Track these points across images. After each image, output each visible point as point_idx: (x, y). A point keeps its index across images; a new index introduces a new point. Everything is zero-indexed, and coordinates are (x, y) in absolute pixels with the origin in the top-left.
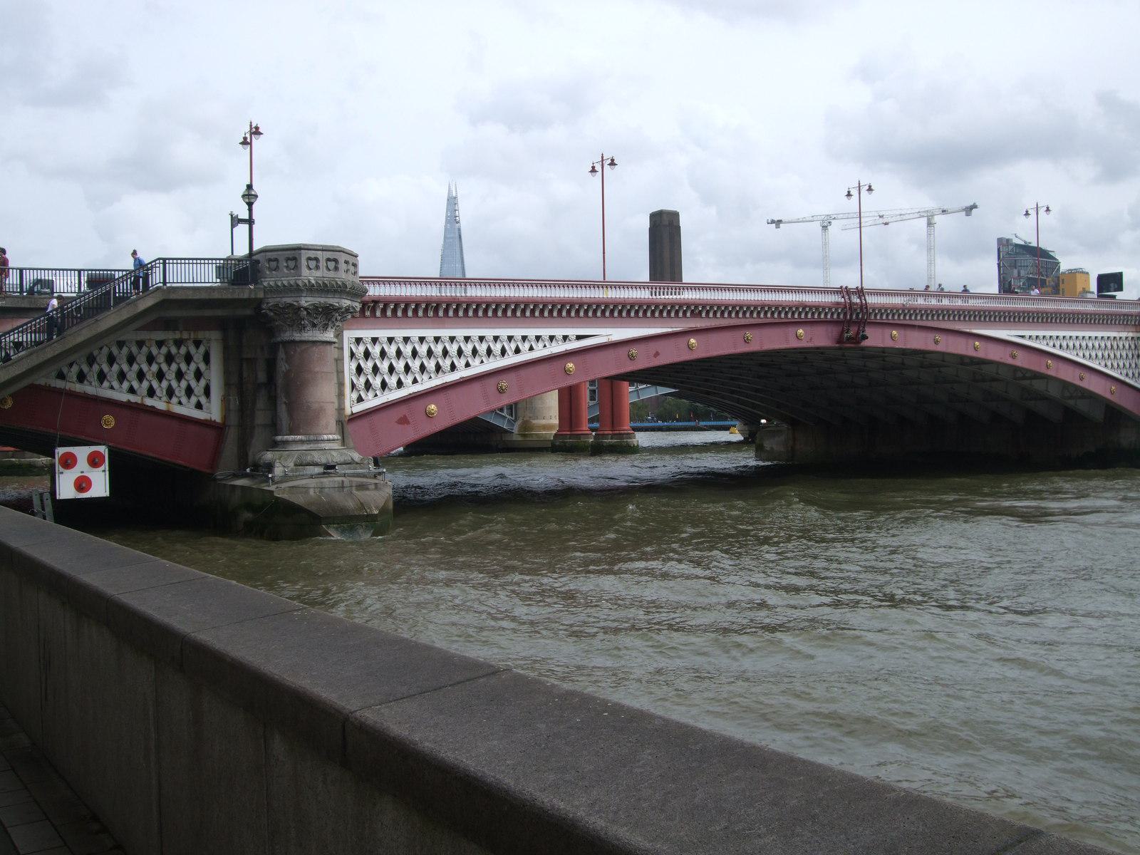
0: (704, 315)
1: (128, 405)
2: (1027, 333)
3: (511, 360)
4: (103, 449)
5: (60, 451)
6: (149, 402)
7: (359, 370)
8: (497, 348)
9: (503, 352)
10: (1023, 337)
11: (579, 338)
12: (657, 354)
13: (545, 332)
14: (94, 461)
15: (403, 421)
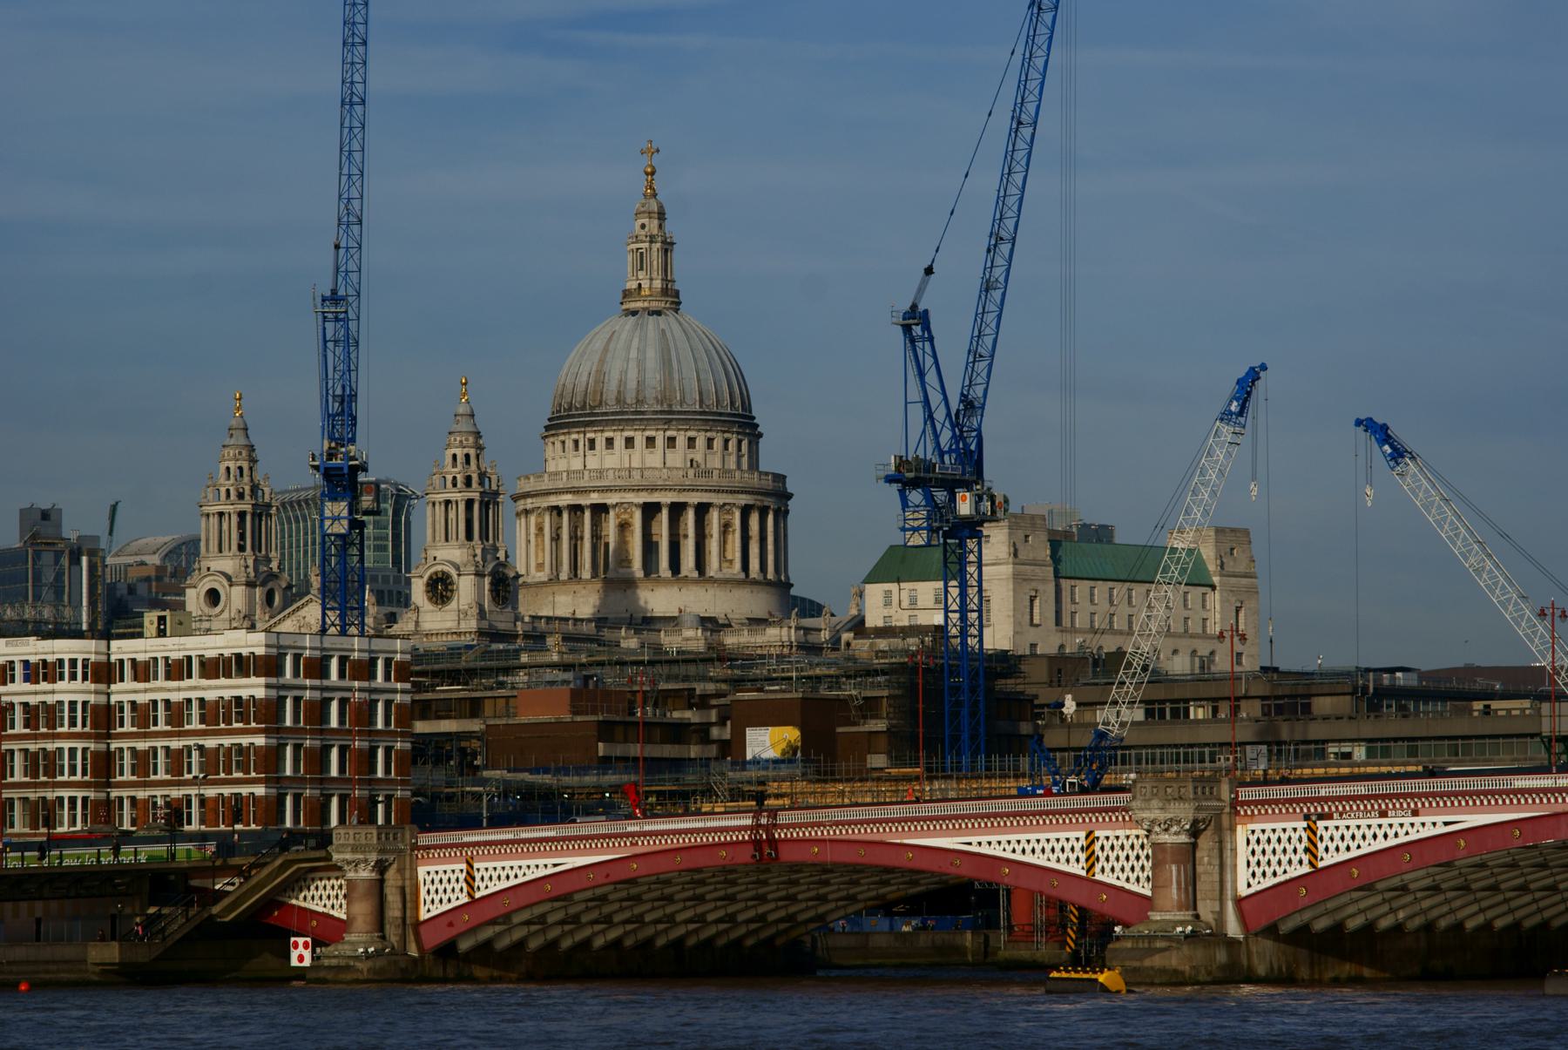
0: (640, 843)
1: (323, 914)
2: (974, 839)
3: (513, 882)
4: (309, 939)
5: (293, 939)
6: (332, 912)
7: (428, 892)
8: (503, 875)
9: (508, 877)
10: (970, 844)
11: (555, 865)
12: (608, 876)
13: (532, 862)
14: (306, 946)
15: (451, 925)
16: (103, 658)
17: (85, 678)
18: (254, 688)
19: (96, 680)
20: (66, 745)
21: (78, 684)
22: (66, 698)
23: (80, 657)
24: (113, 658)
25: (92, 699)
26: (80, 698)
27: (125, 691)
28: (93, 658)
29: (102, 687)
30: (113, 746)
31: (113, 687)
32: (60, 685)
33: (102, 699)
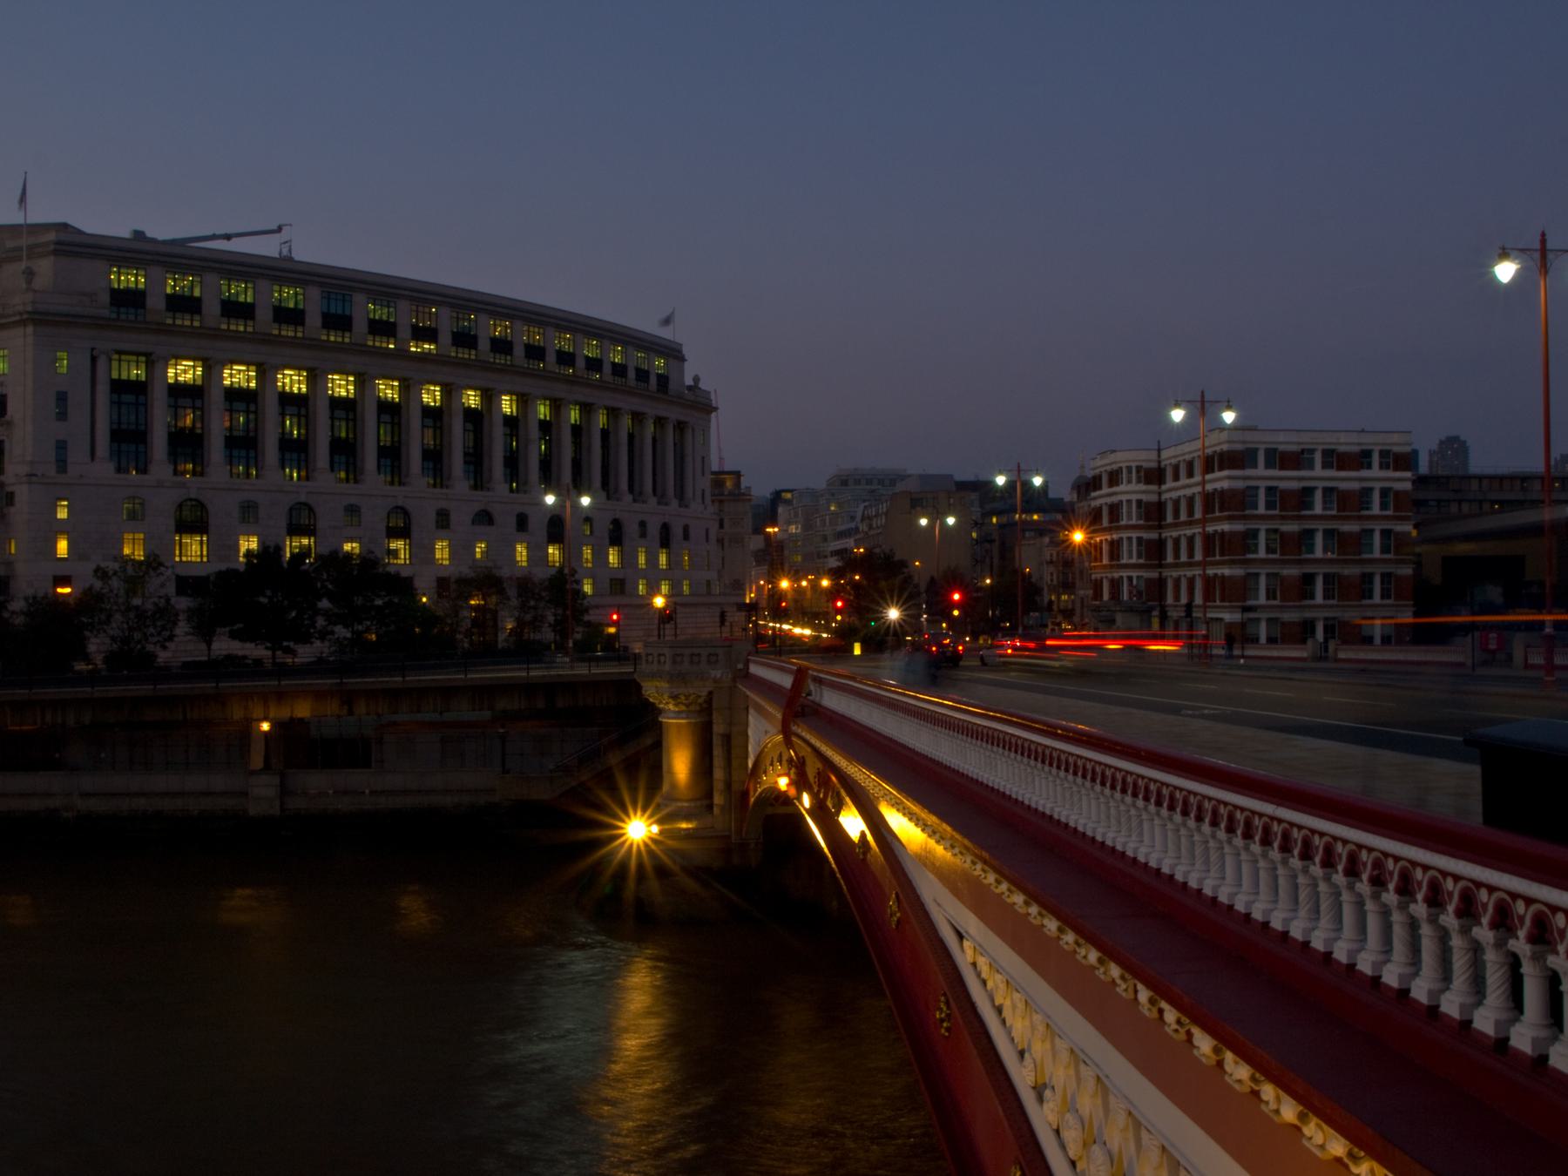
16: (1154, 465)
17: (1139, 481)
18: (1221, 480)
19: (1148, 481)
20: (1124, 535)
21: (1133, 487)
22: (1124, 498)
23: (1134, 465)
24: (1163, 464)
25: (1144, 497)
26: (1134, 497)
27: (1173, 490)
28: (1145, 465)
29: (1154, 488)
30: (1164, 535)
31: (1164, 487)
32: (1122, 488)
33: (1154, 498)
